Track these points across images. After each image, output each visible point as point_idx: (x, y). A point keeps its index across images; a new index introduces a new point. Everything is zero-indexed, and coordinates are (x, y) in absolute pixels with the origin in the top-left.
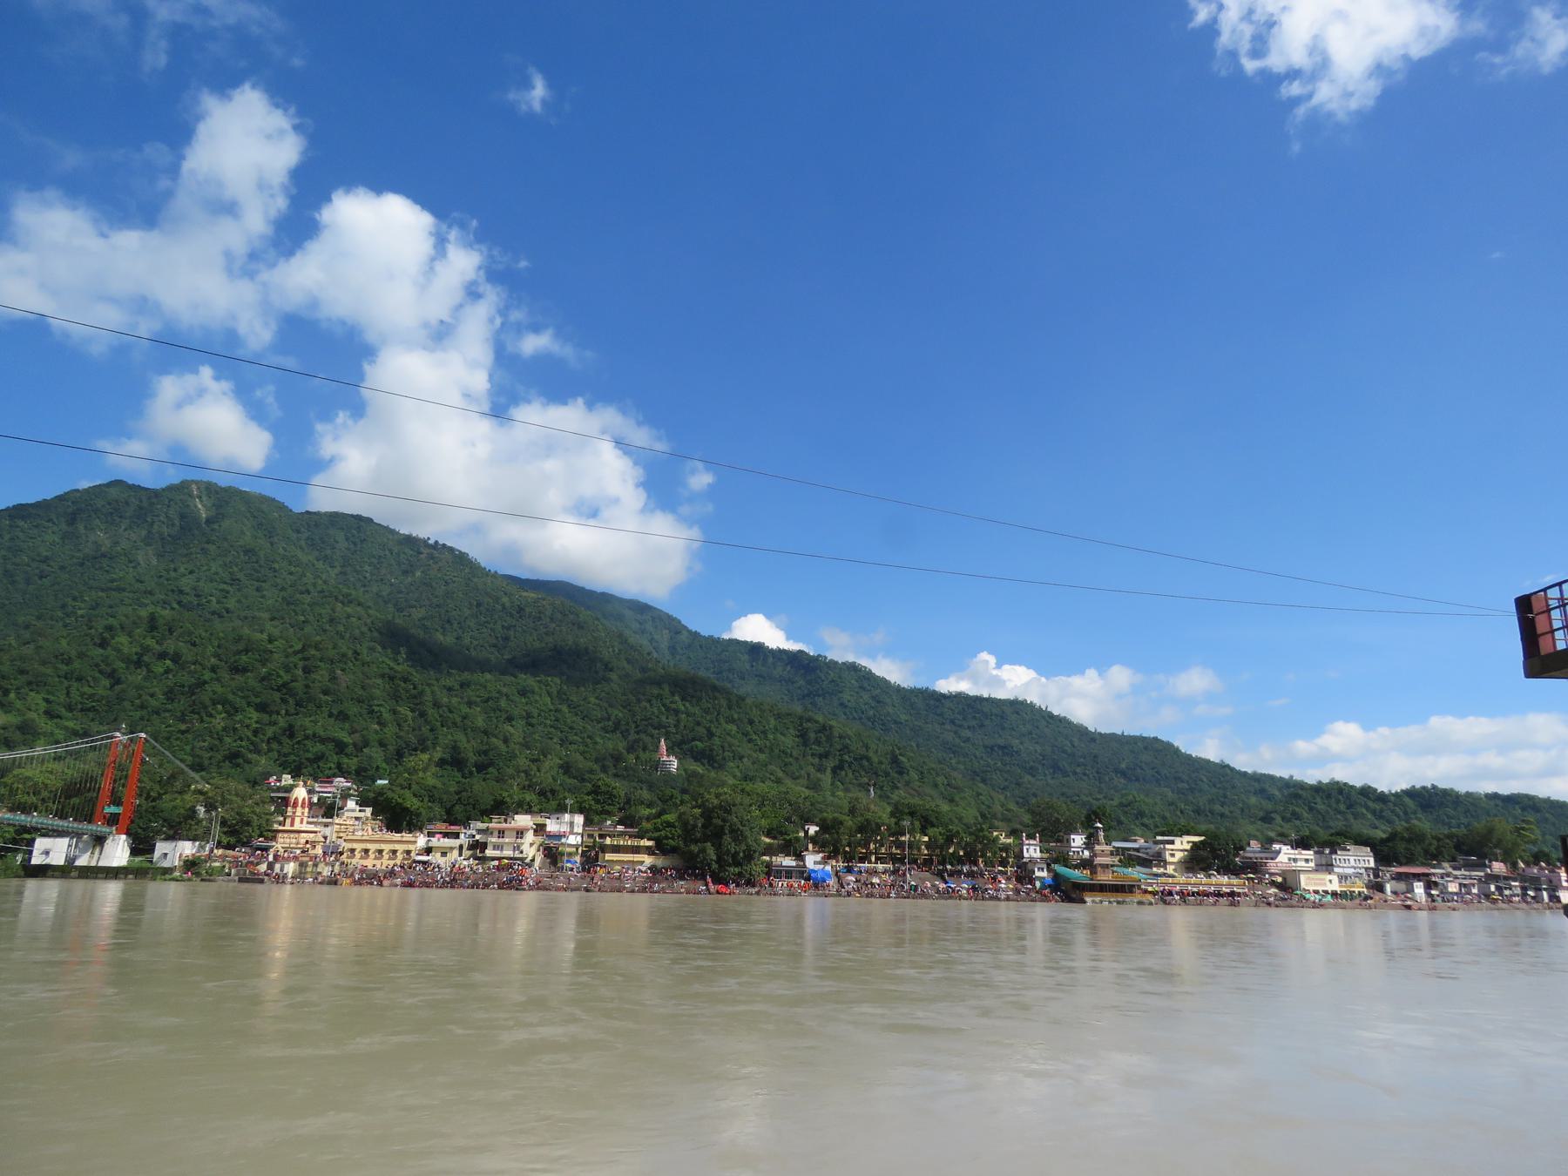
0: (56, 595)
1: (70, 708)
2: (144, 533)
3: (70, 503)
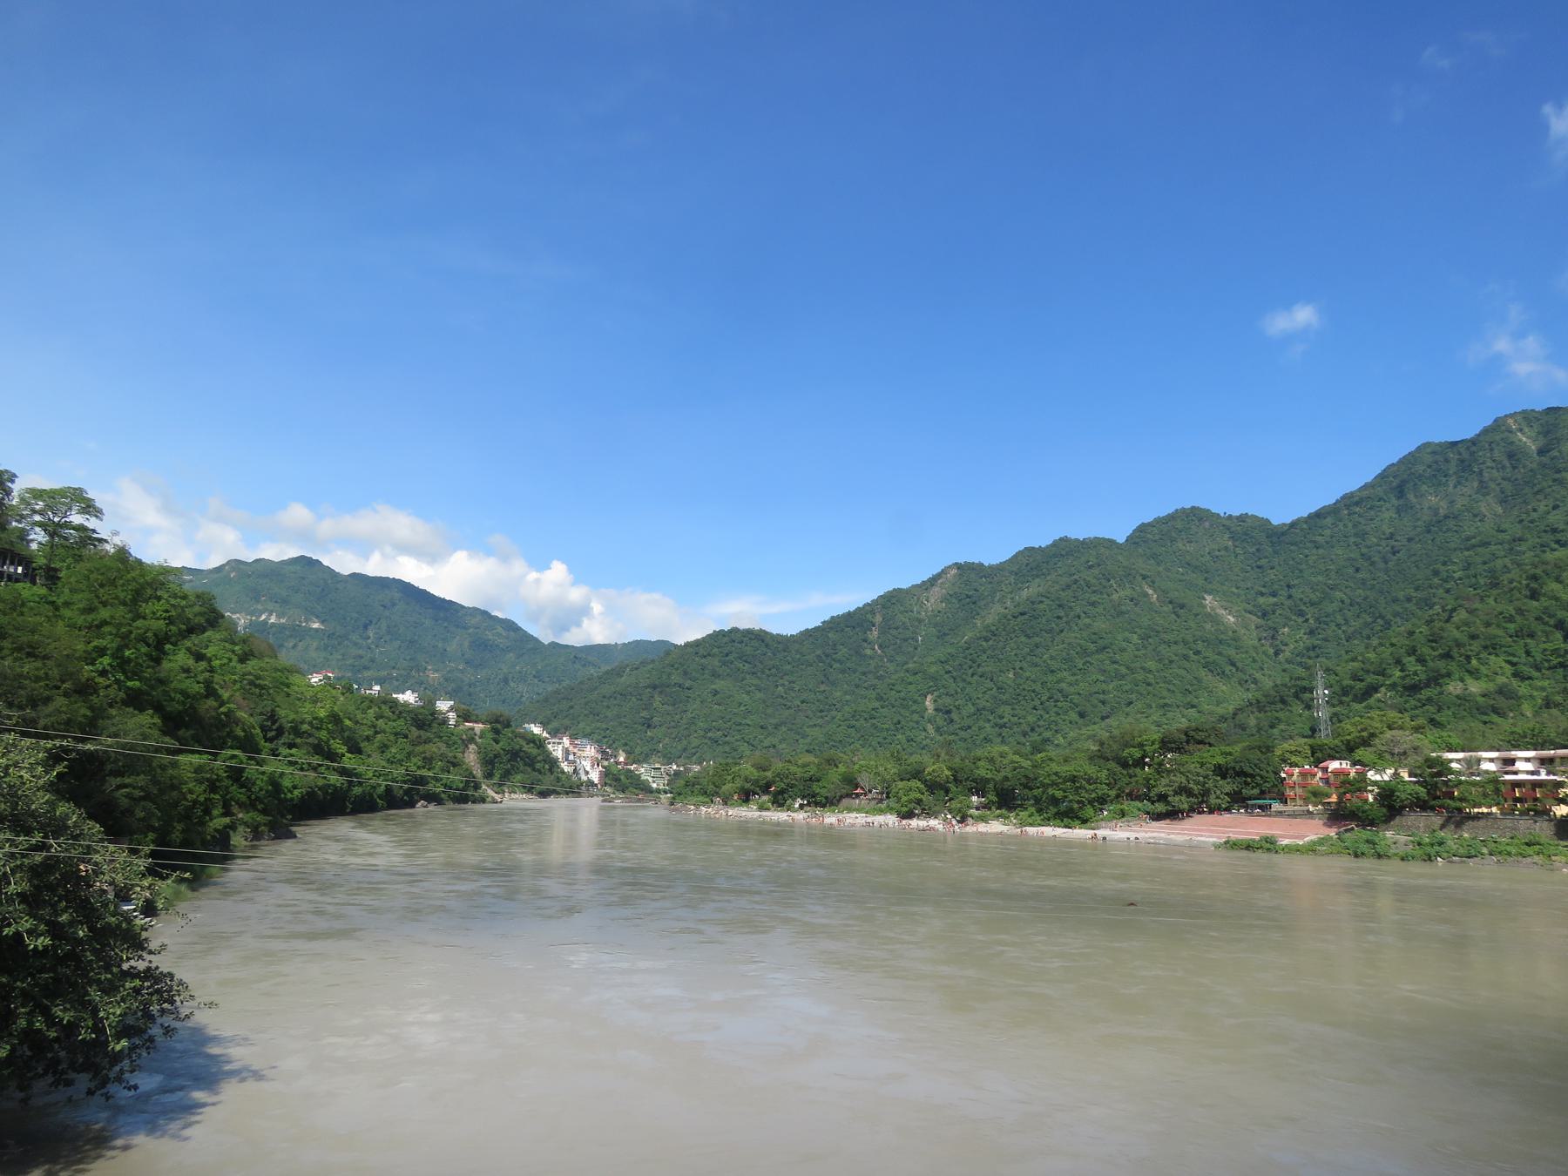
0: (1417, 566)
1: (1538, 669)
2: (1476, 484)
3: (1391, 479)
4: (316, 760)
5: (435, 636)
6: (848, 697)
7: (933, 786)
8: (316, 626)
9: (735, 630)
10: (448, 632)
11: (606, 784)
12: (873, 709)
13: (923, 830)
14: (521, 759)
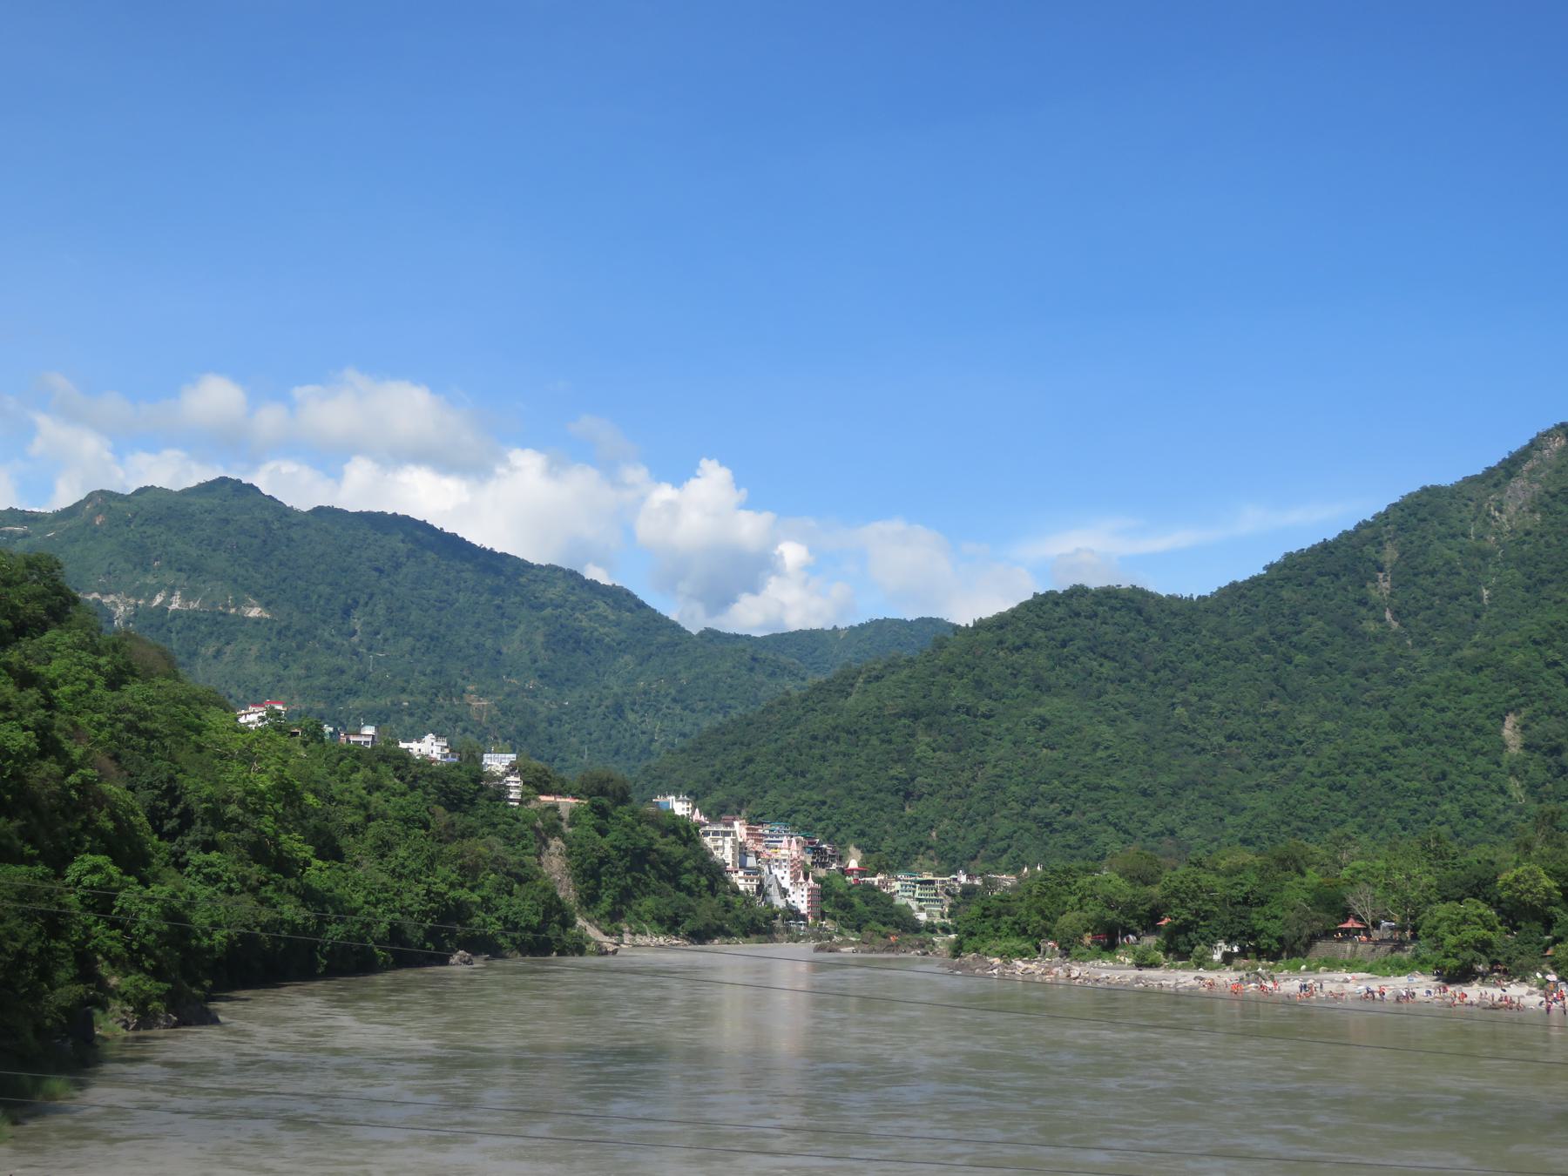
4: (255, 872)
5: (478, 625)
6: (1328, 726)
7: (1516, 913)
8: (254, 613)
9: (1078, 592)
10: (503, 615)
11: (823, 915)
12: (1385, 749)
13: (1494, 1007)
14: (653, 867)
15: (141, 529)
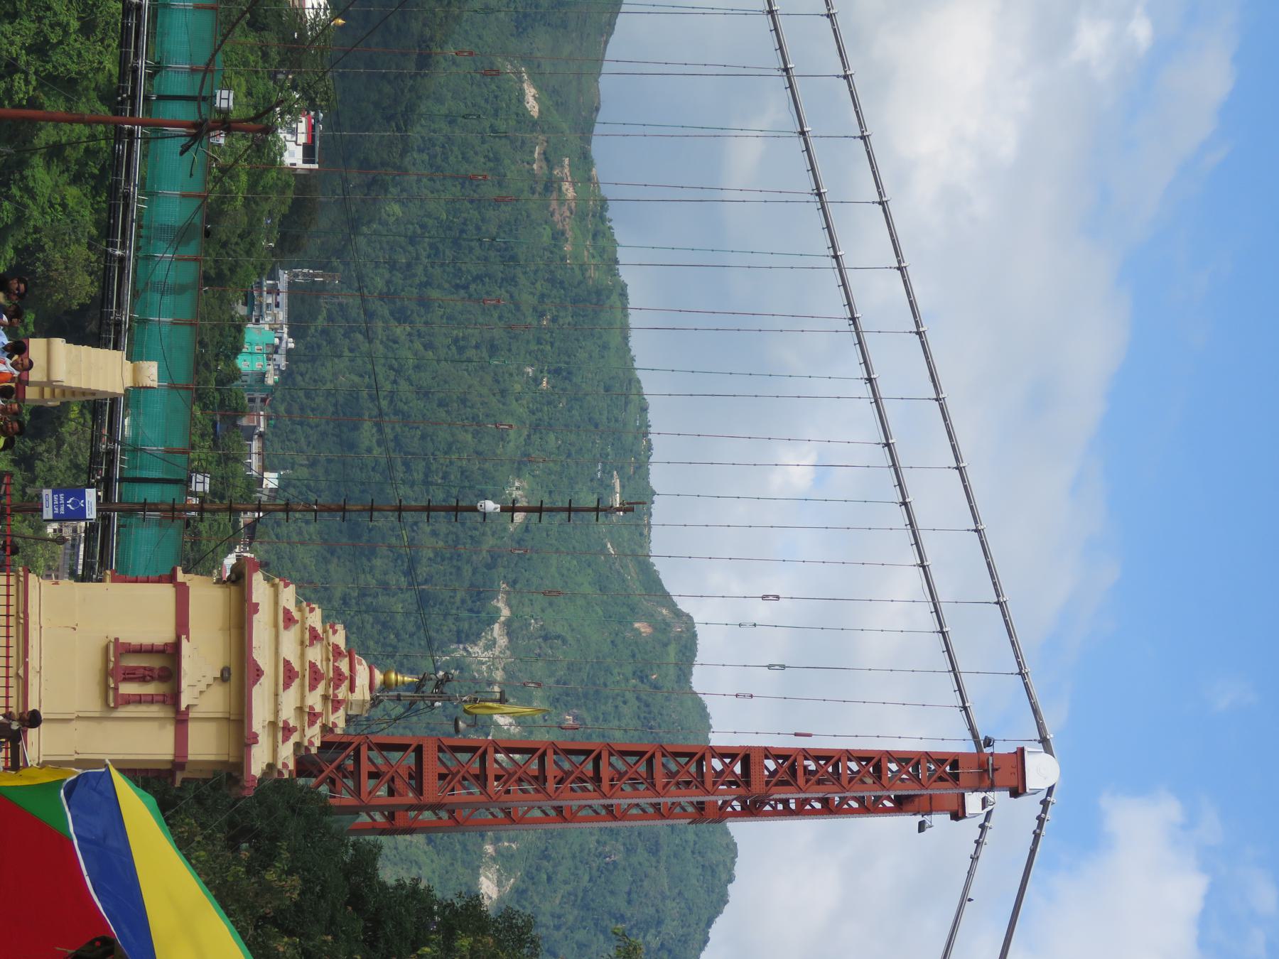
15: (629, 695)
